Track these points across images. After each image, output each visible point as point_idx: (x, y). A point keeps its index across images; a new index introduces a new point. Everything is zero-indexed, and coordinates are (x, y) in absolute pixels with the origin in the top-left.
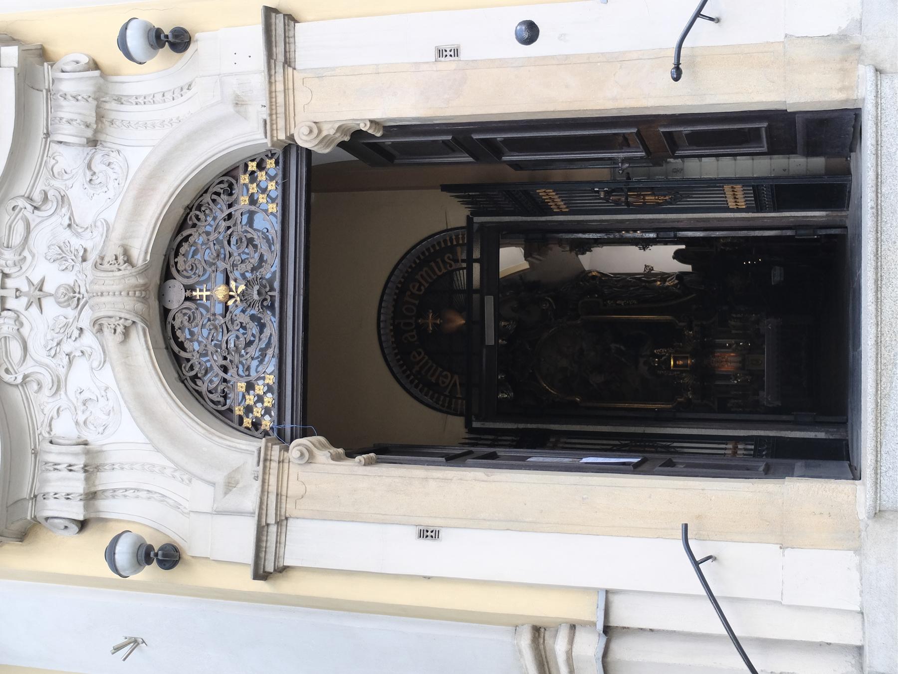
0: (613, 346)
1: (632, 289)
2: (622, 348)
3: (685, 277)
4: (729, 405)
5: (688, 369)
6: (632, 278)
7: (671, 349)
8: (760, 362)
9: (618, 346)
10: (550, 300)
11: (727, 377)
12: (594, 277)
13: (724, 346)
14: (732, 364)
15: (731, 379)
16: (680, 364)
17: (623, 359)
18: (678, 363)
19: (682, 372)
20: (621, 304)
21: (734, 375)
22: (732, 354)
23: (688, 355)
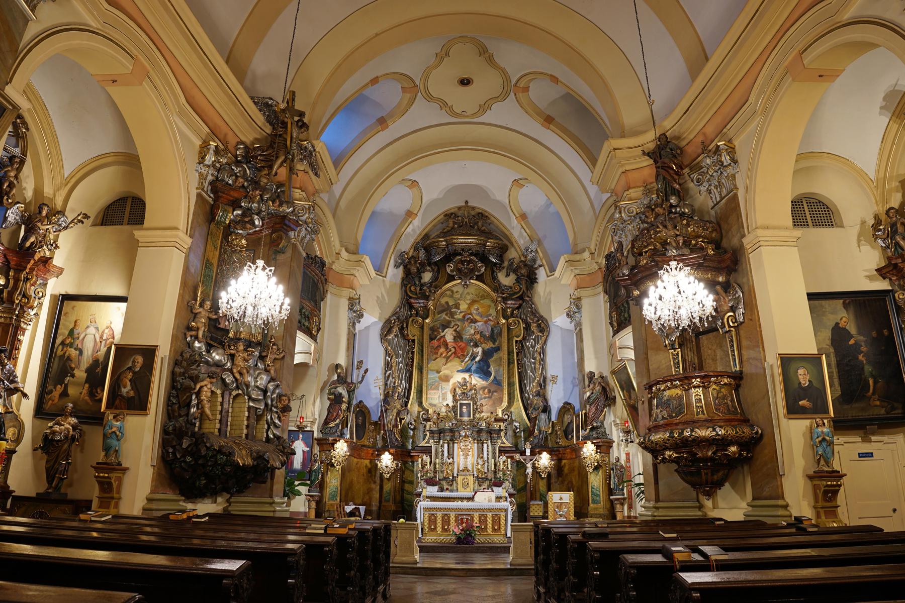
0: (479, 350)
2: (478, 359)
4: (424, 457)
9: (480, 354)
10: (521, 293)
11: (451, 455)
17: (467, 359)
18: (464, 407)
23: (472, 418)
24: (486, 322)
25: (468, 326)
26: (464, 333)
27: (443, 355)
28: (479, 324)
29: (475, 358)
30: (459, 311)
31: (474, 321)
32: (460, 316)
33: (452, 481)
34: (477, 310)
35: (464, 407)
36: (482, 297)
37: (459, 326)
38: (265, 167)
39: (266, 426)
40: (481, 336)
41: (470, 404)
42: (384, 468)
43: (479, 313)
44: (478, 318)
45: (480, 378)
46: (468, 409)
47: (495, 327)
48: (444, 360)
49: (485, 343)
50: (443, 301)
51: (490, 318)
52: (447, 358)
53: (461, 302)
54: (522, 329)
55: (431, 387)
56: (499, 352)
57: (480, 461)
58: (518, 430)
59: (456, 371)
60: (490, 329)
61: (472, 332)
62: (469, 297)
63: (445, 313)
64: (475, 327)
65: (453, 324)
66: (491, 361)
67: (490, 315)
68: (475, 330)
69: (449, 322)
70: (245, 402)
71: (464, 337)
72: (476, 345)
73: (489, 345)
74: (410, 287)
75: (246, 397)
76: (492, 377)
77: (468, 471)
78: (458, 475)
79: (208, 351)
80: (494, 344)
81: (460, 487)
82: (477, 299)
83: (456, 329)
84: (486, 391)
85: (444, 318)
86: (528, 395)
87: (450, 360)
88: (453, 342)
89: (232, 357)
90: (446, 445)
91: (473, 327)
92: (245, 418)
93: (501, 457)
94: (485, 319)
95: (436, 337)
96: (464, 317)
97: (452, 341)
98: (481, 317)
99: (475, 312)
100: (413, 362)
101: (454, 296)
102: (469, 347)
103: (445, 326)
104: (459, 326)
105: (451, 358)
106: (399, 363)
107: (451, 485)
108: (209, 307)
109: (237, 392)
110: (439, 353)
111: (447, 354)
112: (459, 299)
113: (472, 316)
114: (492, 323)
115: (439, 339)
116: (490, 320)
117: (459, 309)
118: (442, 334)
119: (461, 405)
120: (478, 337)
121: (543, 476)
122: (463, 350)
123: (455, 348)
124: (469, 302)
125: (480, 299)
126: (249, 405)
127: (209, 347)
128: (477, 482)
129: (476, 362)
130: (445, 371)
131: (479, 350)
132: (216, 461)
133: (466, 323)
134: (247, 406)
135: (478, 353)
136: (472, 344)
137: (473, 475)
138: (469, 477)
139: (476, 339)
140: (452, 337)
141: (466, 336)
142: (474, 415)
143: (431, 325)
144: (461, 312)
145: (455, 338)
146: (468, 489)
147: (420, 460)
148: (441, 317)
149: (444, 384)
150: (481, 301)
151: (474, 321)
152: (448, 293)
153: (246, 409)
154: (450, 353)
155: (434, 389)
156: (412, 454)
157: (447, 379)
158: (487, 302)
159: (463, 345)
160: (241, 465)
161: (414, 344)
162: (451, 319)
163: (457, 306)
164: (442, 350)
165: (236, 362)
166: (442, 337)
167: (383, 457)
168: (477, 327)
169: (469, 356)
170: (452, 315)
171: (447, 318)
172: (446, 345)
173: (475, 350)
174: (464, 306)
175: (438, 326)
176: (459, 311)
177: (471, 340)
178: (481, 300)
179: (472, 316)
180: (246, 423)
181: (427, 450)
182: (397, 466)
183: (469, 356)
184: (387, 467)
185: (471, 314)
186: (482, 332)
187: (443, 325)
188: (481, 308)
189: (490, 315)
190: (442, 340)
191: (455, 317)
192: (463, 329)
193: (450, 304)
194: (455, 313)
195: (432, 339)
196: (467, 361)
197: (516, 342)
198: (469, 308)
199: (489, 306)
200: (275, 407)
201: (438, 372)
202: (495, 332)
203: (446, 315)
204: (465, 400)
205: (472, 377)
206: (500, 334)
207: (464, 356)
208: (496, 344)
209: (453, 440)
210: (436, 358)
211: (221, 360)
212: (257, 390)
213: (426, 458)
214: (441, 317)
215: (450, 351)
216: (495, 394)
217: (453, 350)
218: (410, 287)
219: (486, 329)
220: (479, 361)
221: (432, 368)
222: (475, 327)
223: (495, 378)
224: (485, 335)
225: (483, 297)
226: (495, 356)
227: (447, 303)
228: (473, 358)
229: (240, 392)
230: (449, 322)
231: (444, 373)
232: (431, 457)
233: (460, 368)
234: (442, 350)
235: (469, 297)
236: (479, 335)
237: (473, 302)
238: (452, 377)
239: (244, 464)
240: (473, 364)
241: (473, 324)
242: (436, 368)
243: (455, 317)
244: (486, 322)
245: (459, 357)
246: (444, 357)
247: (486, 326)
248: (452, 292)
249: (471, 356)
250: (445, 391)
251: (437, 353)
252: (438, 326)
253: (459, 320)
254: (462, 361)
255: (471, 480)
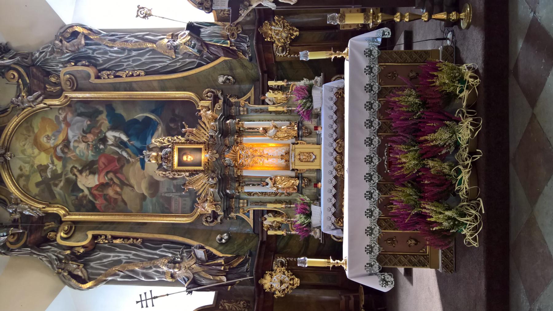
0: (111, 135)
1: (134, 53)
2: (124, 138)
3: (202, 30)
4: (266, 223)
5: (201, 168)
6: (136, 37)
7: (180, 137)
8: (314, 157)
9: (117, 134)
10: (21, 70)
11: (261, 181)
12: (75, 34)
13: (253, 132)
14: (270, 160)
15: (267, 184)
16: (189, 160)
17: (125, 154)
18: (185, 158)
19: (193, 173)
20: (121, 77)
21: (271, 179)
22: (271, 145)
23: (202, 146)
24: (68, 125)
25: (74, 151)
26: (84, 159)
27: (118, 189)
28: (71, 134)
29: (122, 142)
30: (51, 166)
31: (66, 143)
32: (59, 165)
33: (303, 178)
34: (48, 138)
35: (185, 158)
36: (29, 131)
37: (74, 167)
40: (90, 132)
41: (180, 150)
42: (283, 287)
43: (54, 135)
44: (61, 137)
45: (152, 135)
46: (188, 152)
47: (76, 111)
48: (127, 189)
49: (100, 126)
50: (35, 190)
51: (61, 117)
52: (124, 184)
53: (37, 162)
54: (76, 68)
55: (167, 208)
56: (114, 105)
57: (272, 132)
58: (230, 77)
59: (142, 171)
60: (78, 118)
61: (83, 146)
62: (29, 151)
63: (54, 188)
64: (75, 141)
65: (70, 176)
66: (127, 117)
67: (57, 118)
68: (79, 142)
69: (68, 181)
71: (90, 158)
72: (104, 140)
73: (104, 120)
74: (11, 243)
76: (152, 116)
77: (287, 153)
78: (293, 170)
80: (101, 113)
81: (313, 166)
82: (32, 138)
83: (79, 171)
84: (172, 125)
85: (61, 189)
86: (178, 61)
87: (127, 179)
88: (99, 175)
90: (247, 189)
91: (76, 144)
93: (267, 101)
94: (63, 126)
95: (91, 202)
96: (59, 158)
97: (97, 176)
98: (59, 132)
99: (52, 141)
100: (128, 238)
101: (27, 173)
102: (107, 151)
103: (73, 186)
104: (74, 167)
105: (123, 179)
106: (129, 258)
107: (310, 180)
110: (116, 196)
111: (117, 185)
112: (32, 166)
113: (58, 146)
114: (69, 116)
115: (94, 196)
116: (65, 118)
117: (47, 167)
118: (86, 192)
119: (181, 163)
120: (90, 137)
121: (297, 33)
122: (110, 161)
123: (107, 173)
124: (36, 151)
125: (31, 134)
128: (304, 139)
129: (129, 141)
130: (143, 188)
131: (111, 135)
133: (70, 155)
135: (115, 137)
136: (102, 147)
137: (293, 144)
138: (298, 151)
139: (95, 140)
140: (91, 177)
141: (90, 155)
142: (198, 143)
143: (72, 208)
144: (53, 163)
145: (93, 172)
146: (316, 152)
147: (271, 233)
148: (60, 194)
149: (163, 190)
150: (36, 131)
151: (66, 143)
152: (22, 182)
154: (116, 180)
155: (170, 204)
156: (265, 239)
157: (154, 185)
158: (37, 123)
159: (103, 160)
161: (101, 236)
162: (63, 178)
163: (43, 169)
164: (110, 192)
166: (91, 193)
167: (267, 286)
168: (76, 138)
169: (119, 151)
170: (56, 176)
171: (62, 184)
172: (103, 186)
173: (110, 142)
174: (43, 159)
175: (74, 198)
176: (51, 166)
177: (96, 148)
178: (33, 132)
179: (58, 146)
181: (259, 215)
182: (282, 264)
183: (119, 151)
184: (282, 283)
185: (55, 148)
186: (84, 131)
187: (73, 191)
188: (46, 131)
189: (57, 118)
190: (95, 192)
191: (59, 171)
192: (78, 160)
193: (39, 179)
194: (54, 172)
195: (93, 209)
196: (128, 153)
197: (98, 77)
198: (46, 150)
199: (43, 119)
201: (144, 198)
202: (82, 110)
203: (56, 185)
204: (173, 157)
205: (151, 146)
206: (85, 102)
207: (121, 157)
208: (101, 108)
209: (240, 180)
210: (123, 201)
213: (269, 220)
214: (60, 194)
215: (111, 179)
216: (177, 112)
217: (111, 175)
218: (11, 243)
219: (79, 124)
220: (128, 135)
221: (139, 207)
222: (75, 141)
223: (153, 112)
224: (89, 126)
225: (30, 128)
226: (120, 110)
227: (38, 184)
228: (121, 144)
230: (68, 181)
231: (146, 188)
232: (269, 212)
233: (138, 164)
234: (110, 192)
235: (29, 151)
236: (88, 136)
237: (37, 144)
238: (152, 177)
240: (132, 144)
241: (72, 144)
242: (138, 201)
243: (59, 171)
244: (68, 125)
245: (122, 167)
246: (122, 189)
247: (75, 124)
248: (20, 176)
249: (120, 148)
250: (172, 187)
251: (115, 199)
252: (74, 198)
253: (64, 166)
254: (128, 161)
255: (302, 148)
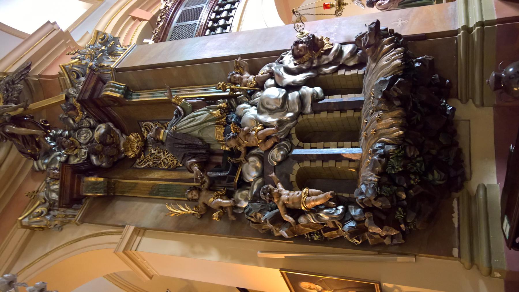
38: (36, 140)
39: (341, 72)
70: (308, 119)
75: (300, 119)
79: (249, 184)
89: (249, 149)
92: (330, 115)
108: (194, 193)
109: (294, 136)
126: (311, 113)
127: (243, 184)
132: (399, 173)
134: (311, 117)
153: (317, 116)
160: (401, 132)
165: (254, 144)
180: (337, 114)
200: (312, 63)
211: (256, 168)
212: (287, 105)
229: (293, 131)
239: (401, 127)
